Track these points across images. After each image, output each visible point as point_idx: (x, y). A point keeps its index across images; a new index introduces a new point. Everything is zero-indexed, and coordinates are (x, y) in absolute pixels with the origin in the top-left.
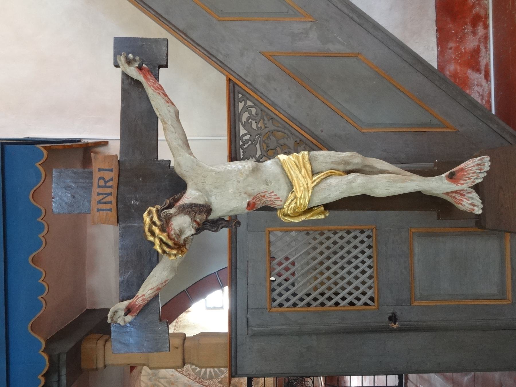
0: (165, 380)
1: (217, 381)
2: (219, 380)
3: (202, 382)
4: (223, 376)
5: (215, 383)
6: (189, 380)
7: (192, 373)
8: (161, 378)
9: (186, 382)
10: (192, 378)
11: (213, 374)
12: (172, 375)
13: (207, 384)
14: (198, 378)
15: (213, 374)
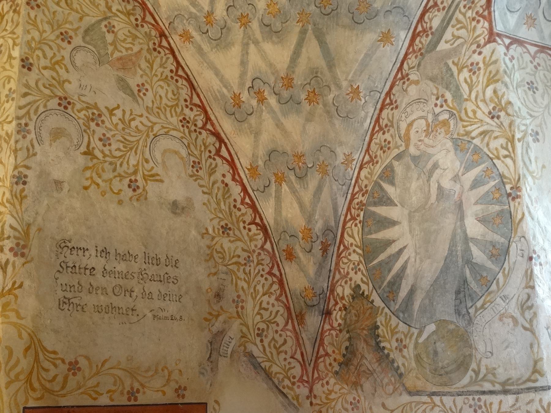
0: (321, 63)
1: (357, 278)
2: (364, 287)
3: (353, 218)
4: (378, 302)
5: (352, 274)
6: (356, 165)
7: (378, 169)
8: (322, 43)
9: (341, 152)
10: (363, 173)
11: (382, 257)
12: (356, 92)
13: (348, 240)
14: (364, 199)
15: (382, 257)
